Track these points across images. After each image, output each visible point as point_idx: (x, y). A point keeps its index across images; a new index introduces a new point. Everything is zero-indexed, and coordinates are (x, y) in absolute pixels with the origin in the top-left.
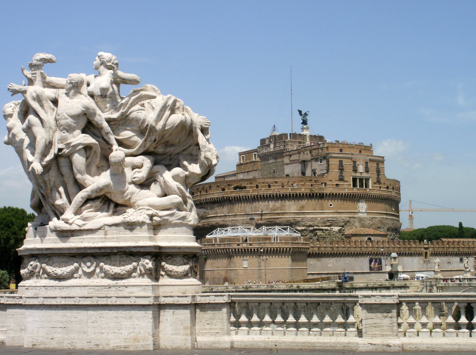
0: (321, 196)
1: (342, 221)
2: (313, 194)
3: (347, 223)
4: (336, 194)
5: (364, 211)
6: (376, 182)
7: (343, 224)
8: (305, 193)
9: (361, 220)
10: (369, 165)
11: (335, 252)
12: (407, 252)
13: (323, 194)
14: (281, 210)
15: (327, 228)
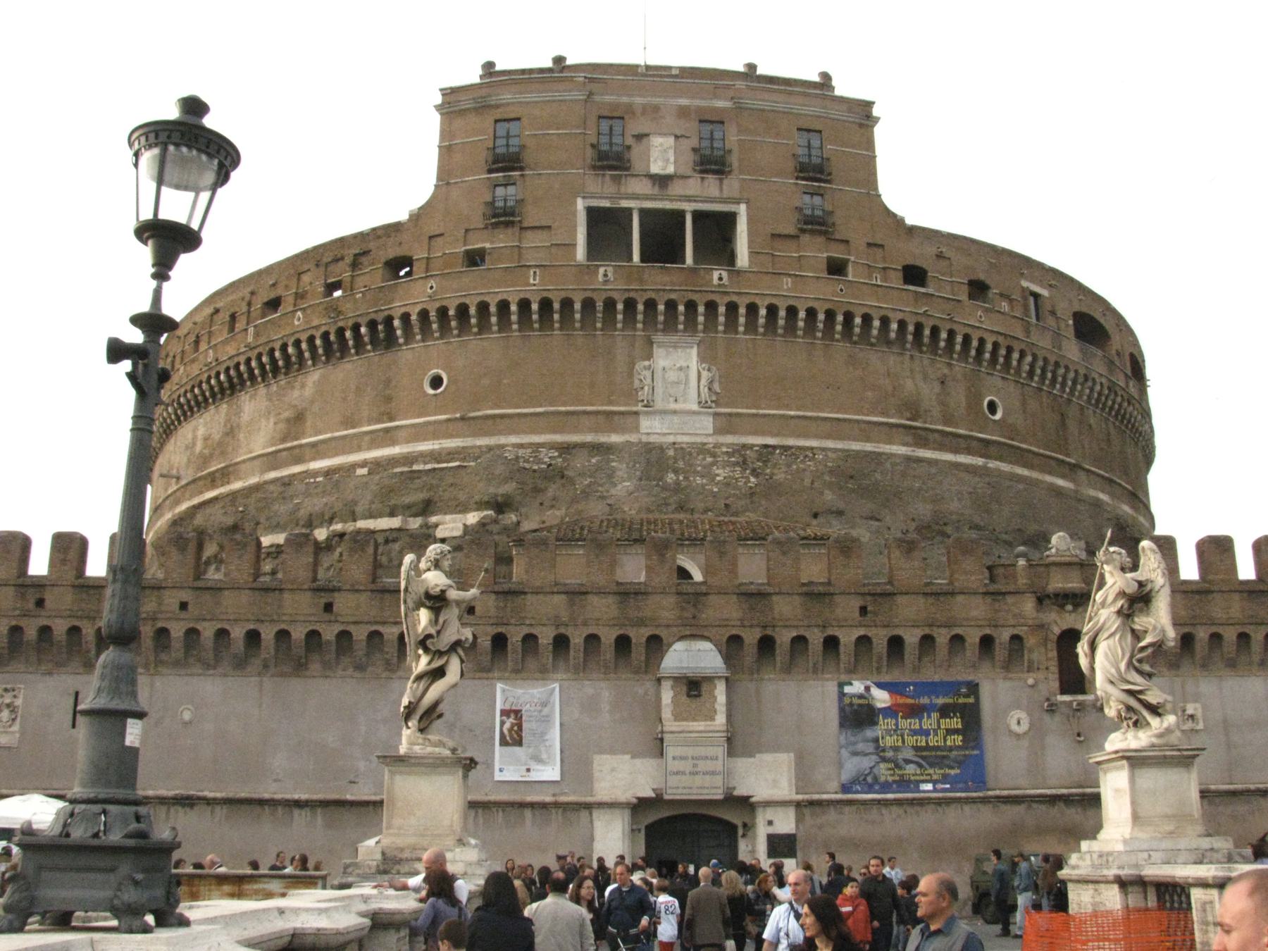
0: (383, 335)
1: (500, 469)
2: (340, 332)
3: (538, 480)
4: (463, 310)
5: (695, 407)
6: (791, 230)
7: (509, 488)
8: (304, 337)
9: (654, 459)
10: (733, 137)
11: (60, 627)
12: (847, 638)
13: (389, 320)
14: (223, 453)
15: (395, 522)
